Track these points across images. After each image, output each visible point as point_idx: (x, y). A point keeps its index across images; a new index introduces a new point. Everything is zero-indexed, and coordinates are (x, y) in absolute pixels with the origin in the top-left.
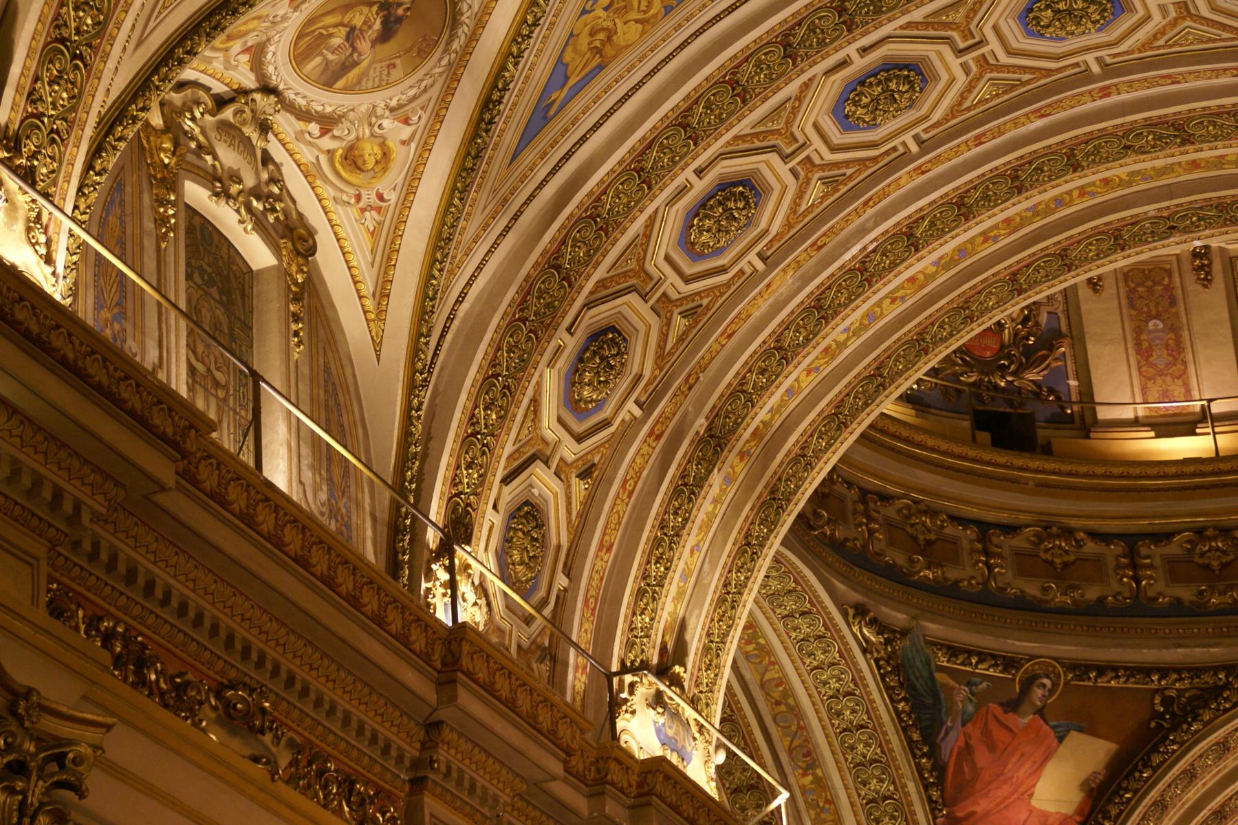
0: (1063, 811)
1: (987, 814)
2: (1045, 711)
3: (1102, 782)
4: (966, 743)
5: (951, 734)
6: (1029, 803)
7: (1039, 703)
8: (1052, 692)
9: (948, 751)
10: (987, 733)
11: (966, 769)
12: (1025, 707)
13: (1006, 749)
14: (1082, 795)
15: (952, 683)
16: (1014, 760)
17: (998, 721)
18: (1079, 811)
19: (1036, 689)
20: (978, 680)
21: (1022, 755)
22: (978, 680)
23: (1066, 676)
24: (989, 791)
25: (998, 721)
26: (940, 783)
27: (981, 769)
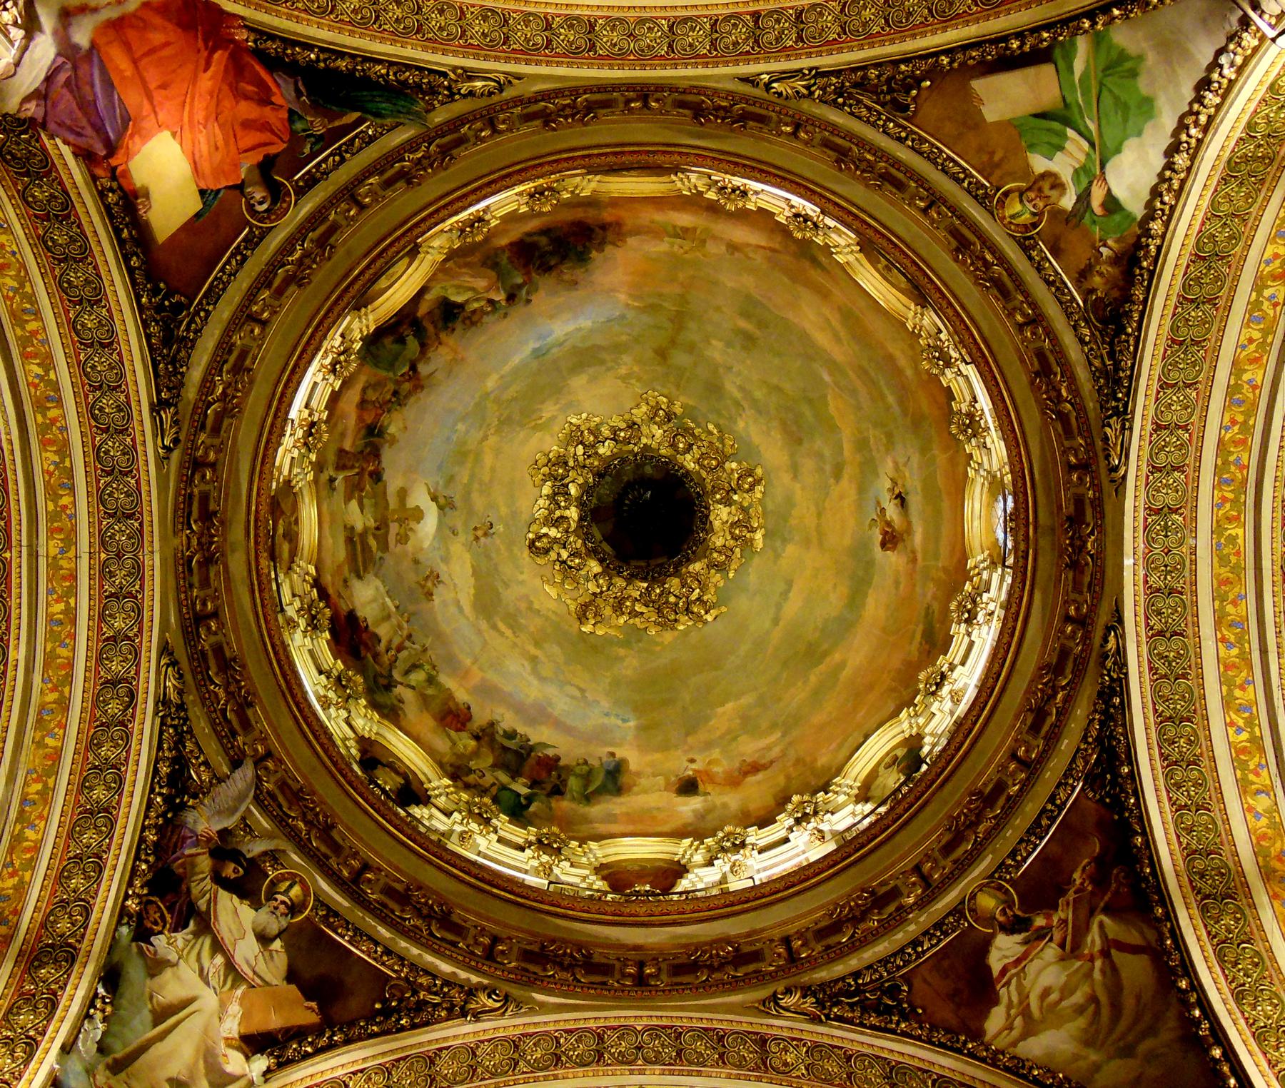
0: (137, 158)
1: (194, 79)
2: (237, 192)
3: (137, 210)
4: (272, 103)
5: (293, 94)
6: (168, 127)
7: (249, 190)
8: (251, 208)
9: (279, 81)
10: (265, 127)
11: (250, 88)
12: (256, 175)
13: (235, 136)
14: (138, 185)
15: (337, 123)
16: (220, 137)
17: (265, 144)
18: (126, 173)
19: (264, 194)
20: (317, 147)
21: (217, 148)
22: (317, 147)
23: (258, 227)
24: (212, 97)
25: (265, 144)
26: (260, 54)
27: (237, 102)
